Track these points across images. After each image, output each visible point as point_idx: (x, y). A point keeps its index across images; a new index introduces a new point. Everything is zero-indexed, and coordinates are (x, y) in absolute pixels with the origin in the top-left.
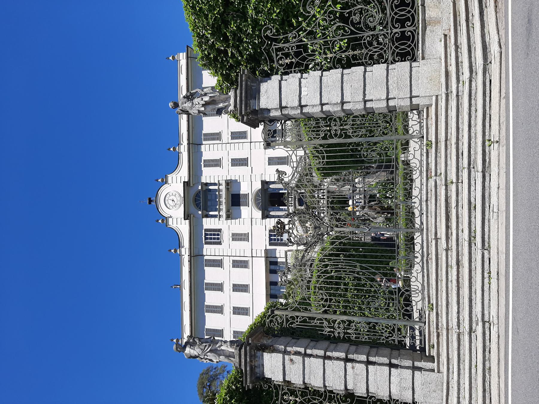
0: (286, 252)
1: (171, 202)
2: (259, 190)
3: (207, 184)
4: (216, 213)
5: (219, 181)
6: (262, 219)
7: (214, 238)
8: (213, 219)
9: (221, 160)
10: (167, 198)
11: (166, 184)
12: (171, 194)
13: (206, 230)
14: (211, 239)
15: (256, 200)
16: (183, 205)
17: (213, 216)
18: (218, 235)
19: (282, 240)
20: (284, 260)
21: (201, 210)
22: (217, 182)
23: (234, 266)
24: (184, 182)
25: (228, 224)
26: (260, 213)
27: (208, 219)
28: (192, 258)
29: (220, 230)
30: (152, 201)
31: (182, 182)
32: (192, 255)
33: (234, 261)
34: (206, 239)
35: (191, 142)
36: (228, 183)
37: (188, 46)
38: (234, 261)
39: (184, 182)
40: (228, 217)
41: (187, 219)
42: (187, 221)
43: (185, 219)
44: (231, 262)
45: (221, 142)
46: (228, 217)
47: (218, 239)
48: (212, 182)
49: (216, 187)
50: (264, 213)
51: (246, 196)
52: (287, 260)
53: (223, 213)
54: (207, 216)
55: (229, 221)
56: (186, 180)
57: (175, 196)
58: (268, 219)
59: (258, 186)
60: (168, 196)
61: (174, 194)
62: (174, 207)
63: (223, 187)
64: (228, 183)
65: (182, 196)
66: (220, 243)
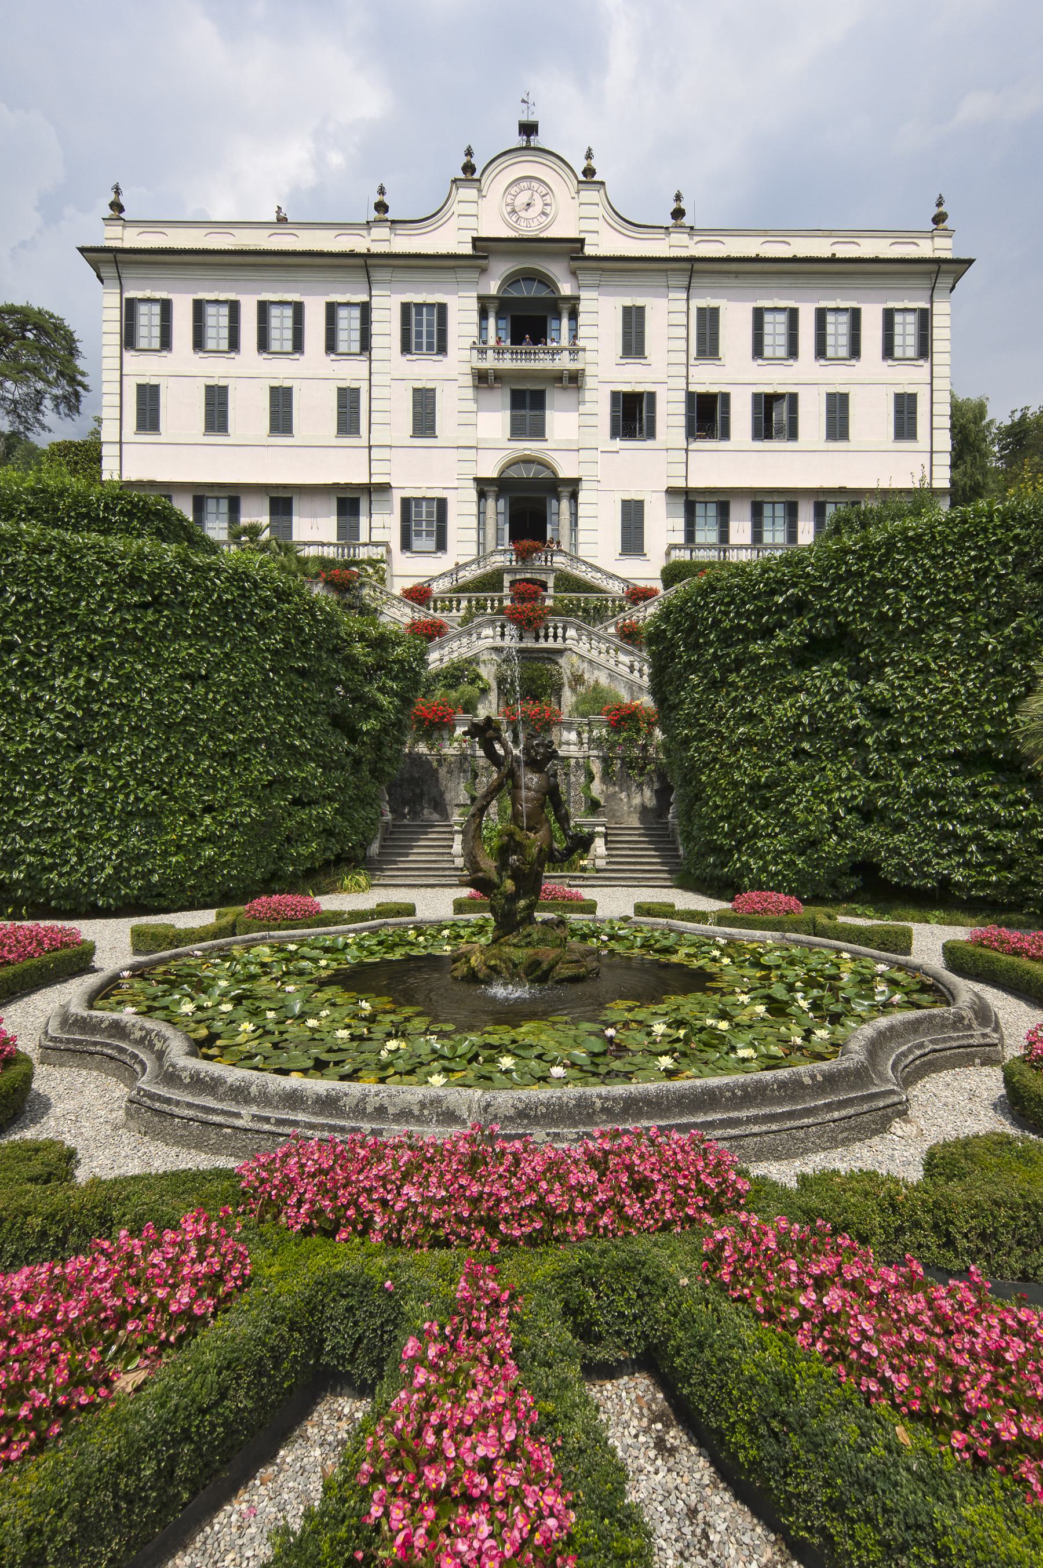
0: (386, 544)
1: (523, 198)
2: (554, 472)
3: (574, 315)
4: (492, 341)
5: (584, 350)
6: (475, 479)
7: (419, 335)
8: (474, 330)
9: (642, 361)
10: (535, 185)
11: (579, 182)
12: (548, 201)
13: (442, 308)
14: (419, 323)
15: (528, 461)
16: (512, 234)
17: (482, 329)
18: (430, 347)
19: (419, 534)
20: (364, 538)
21: (501, 295)
22: (581, 343)
23: (342, 392)
24: (582, 241)
25: (461, 378)
26: (492, 473)
27: (475, 317)
28: (360, 261)
29: (442, 349)
30: (528, 136)
31: (582, 236)
32: (370, 262)
33: (356, 391)
34: (419, 306)
35: (698, 266)
36: (574, 380)
37: (970, 262)
38: (356, 391)
39: (582, 241)
40: (483, 379)
41: (474, 247)
42: (467, 249)
43: (475, 240)
44: (354, 385)
45: (692, 361)
46: (483, 379)
47: (419, 346)
48: (582, 332)
49: (565, 342)
50: (491, 485)
51: (538, 431)
52: (366, 545)
53: (490, 362)
54: (483, 315)
55: (468, 381)
56: (588, 251)
57: (544, 213)
58: (473, 495)
59: (565, 471)
60: (543, 190)
61: (548, 210)
62: (509, 209)
63: (564, 362)
64: (574, 380)
65: (542, 235)
66: (406, 349)
